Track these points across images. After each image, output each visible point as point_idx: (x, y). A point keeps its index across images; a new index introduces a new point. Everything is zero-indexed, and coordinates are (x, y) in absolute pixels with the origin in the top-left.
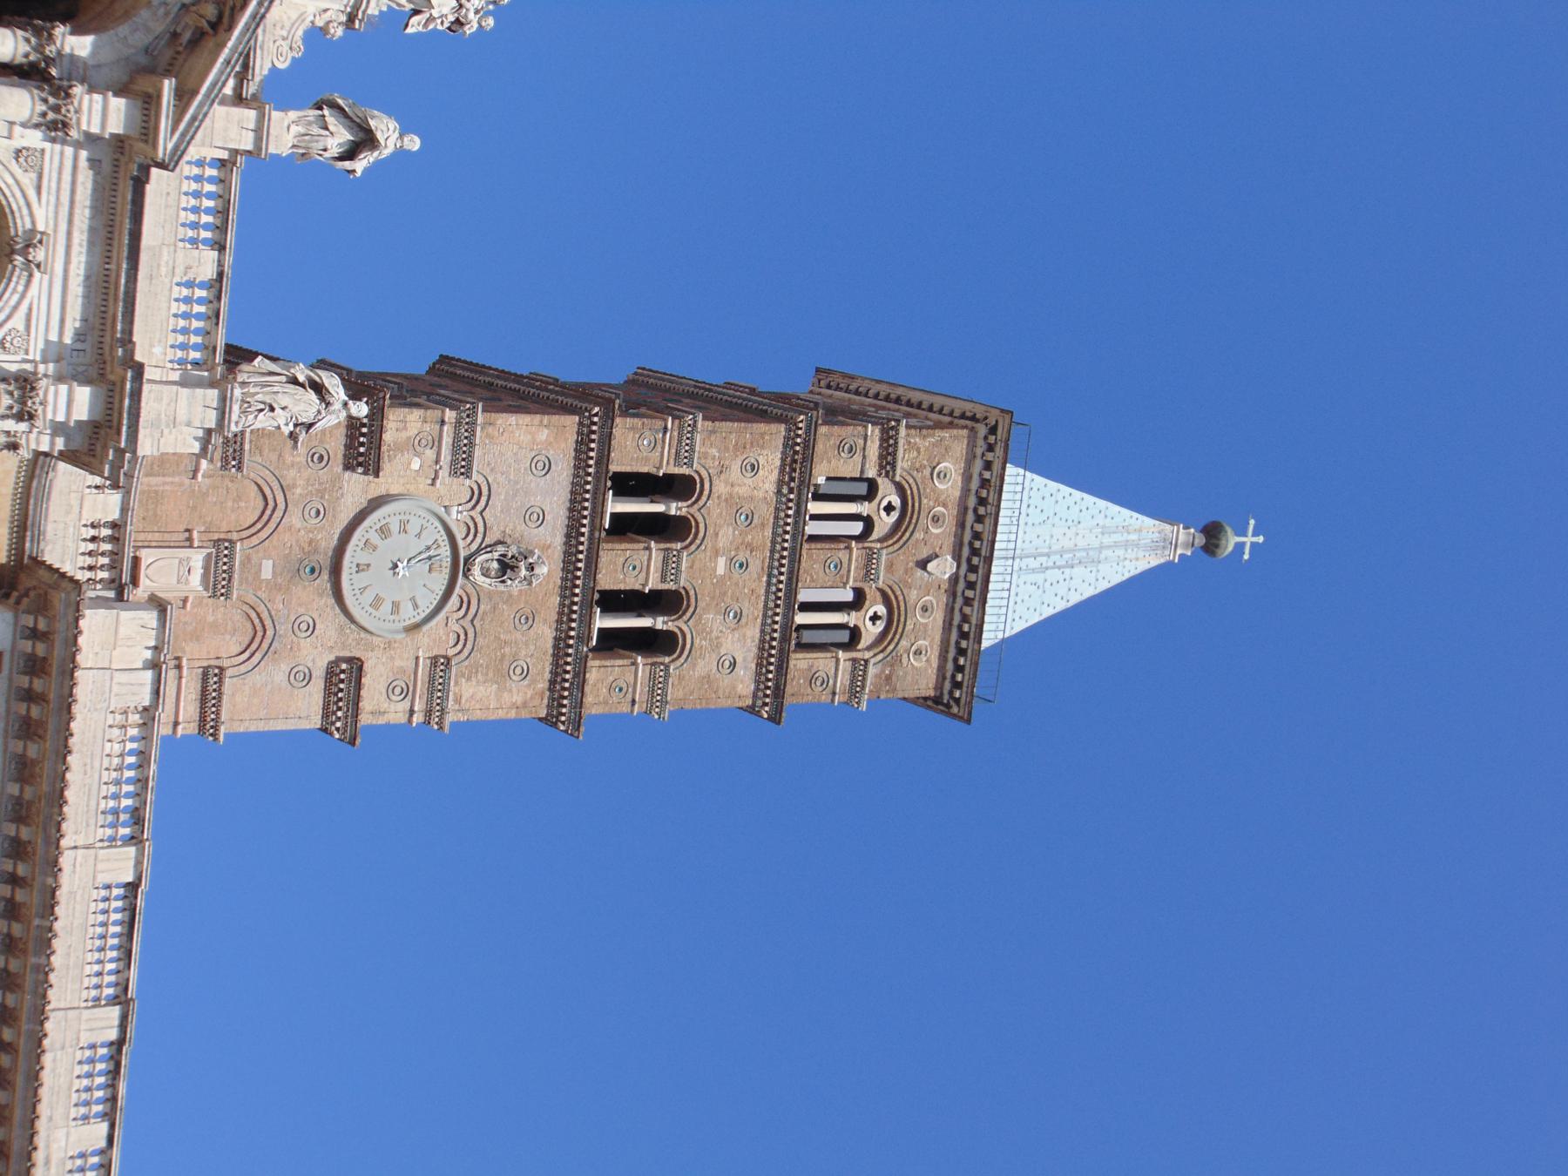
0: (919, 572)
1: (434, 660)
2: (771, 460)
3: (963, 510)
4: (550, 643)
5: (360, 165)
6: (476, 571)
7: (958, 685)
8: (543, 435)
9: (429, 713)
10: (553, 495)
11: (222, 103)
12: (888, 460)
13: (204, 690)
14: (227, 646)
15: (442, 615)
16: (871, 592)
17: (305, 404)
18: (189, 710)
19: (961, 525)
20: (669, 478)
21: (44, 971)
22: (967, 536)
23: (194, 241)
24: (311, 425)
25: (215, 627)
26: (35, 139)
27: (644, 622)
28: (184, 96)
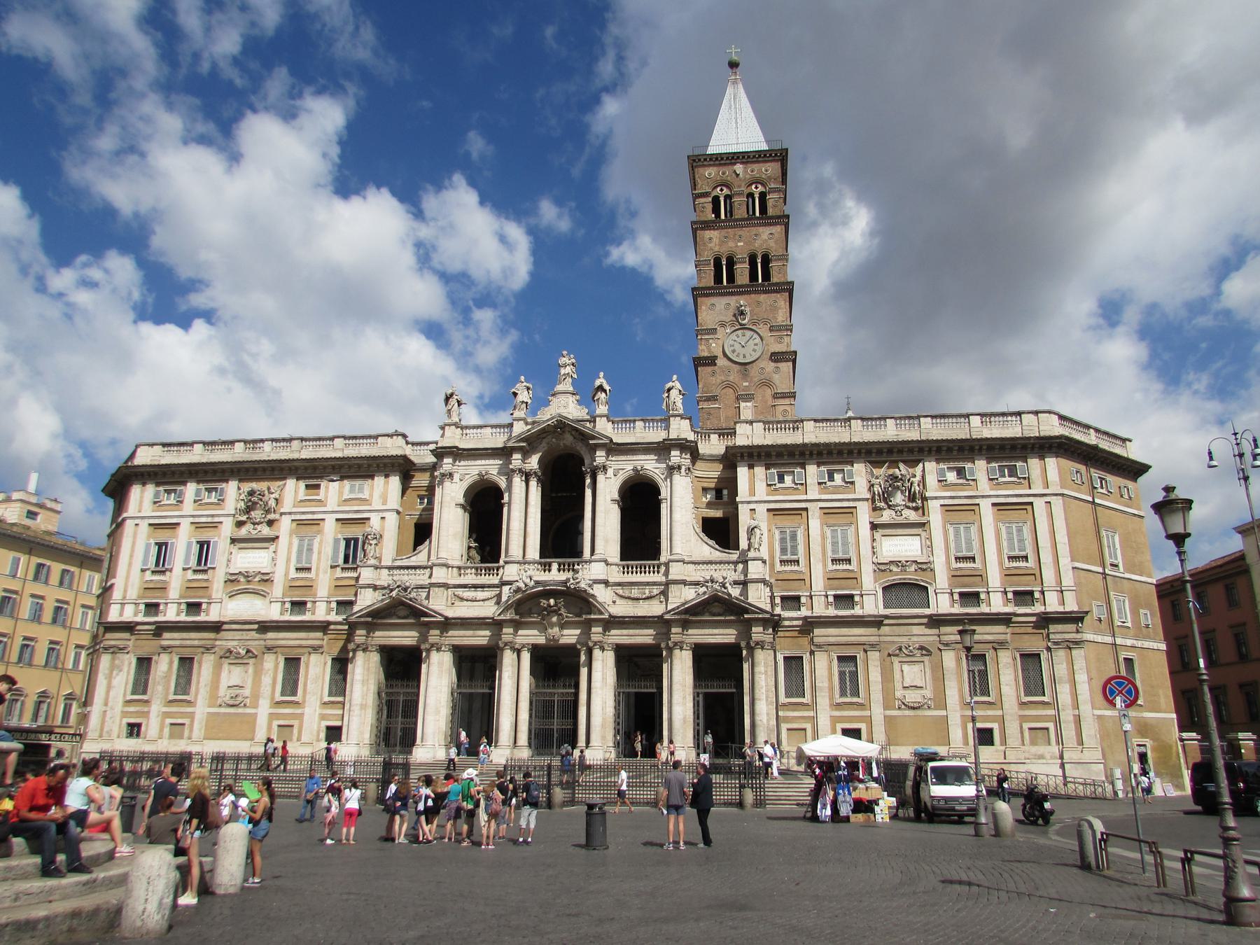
0: (741, 176)
1: (771, 330)
2: (708, 234)
3: (720, 165)
4: (766, 295)
5: (607, 388)
6: (744, 322)
7: (776, 155)
8: (703, 308)
9: (787, 330)
10: (720, 302)
11: (594, 427)
12: (705, 195)
13: (781, 398)
14: (769, 392)
15: (758, 330)
16: (747, 191)
17: (674, 393)
18: (787, 401)
19: (725, 164)
20: (715, 266)
21: (836, 444)
22: (728, 162)
23: (634, 428)
24: (680, 391)
25: (763, 397)
26: (610, 472)
27: (759, 265)
28: (594, 438)
